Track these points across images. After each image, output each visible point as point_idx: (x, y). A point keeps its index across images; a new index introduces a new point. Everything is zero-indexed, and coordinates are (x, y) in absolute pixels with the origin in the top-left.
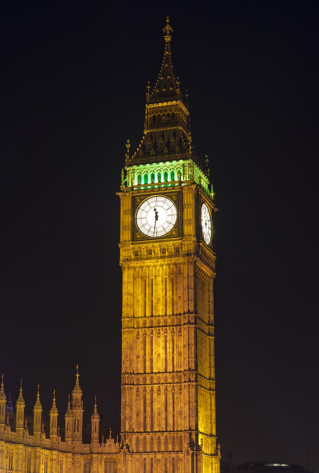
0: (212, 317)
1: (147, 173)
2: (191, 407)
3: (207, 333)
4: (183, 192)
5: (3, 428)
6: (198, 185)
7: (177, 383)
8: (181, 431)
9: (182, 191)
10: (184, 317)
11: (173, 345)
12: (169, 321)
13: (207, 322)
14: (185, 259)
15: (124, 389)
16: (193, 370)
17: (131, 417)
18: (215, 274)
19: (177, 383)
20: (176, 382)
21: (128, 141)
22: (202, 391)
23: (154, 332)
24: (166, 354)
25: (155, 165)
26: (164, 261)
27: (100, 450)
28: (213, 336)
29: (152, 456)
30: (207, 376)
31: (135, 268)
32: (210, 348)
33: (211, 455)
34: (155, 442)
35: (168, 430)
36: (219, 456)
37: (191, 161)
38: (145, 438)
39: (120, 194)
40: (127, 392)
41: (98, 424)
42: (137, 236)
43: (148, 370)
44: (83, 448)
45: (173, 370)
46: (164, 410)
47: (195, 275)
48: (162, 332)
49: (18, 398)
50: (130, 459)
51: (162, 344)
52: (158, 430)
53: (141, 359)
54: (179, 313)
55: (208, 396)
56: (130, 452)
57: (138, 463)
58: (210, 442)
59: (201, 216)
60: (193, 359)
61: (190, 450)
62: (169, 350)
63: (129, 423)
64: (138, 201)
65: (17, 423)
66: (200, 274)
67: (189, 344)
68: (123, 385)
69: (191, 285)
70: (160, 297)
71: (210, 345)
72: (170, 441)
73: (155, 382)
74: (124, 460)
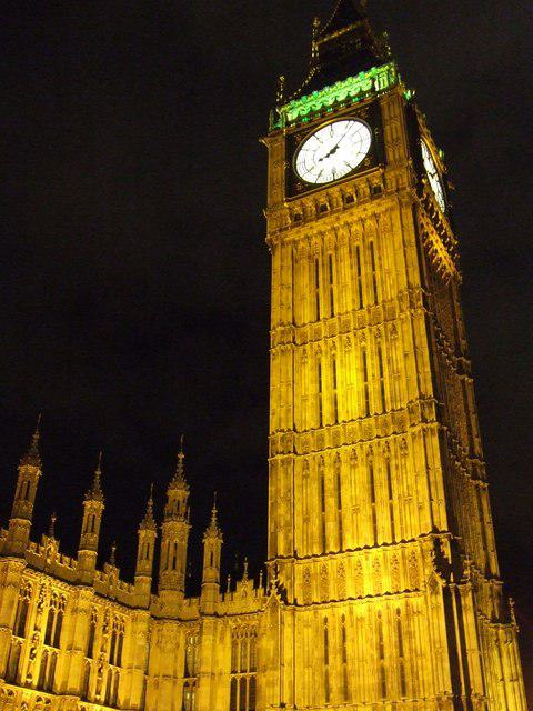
14: (393, 200)
16: (430, 397)
17: (290, 525)
23: (338, 345)
24: (366, 380)
26: (352, 214)
27: (221, 609)
29: (342, 609)
31: (295, 243)
32: (466, 397)
38: (324, 570)
39: (268, 139)
40: (281, 469)
41: (217, 550)
42: (295, 186)
43: (327, 419)
50: (288, 619)
52: (356, 546)
53: (311, 401)
56: (287, 604)
60: (429, 376)
62: (372, 370)
63: (286, 537)
68: (273, 456)
73: (342, 441)
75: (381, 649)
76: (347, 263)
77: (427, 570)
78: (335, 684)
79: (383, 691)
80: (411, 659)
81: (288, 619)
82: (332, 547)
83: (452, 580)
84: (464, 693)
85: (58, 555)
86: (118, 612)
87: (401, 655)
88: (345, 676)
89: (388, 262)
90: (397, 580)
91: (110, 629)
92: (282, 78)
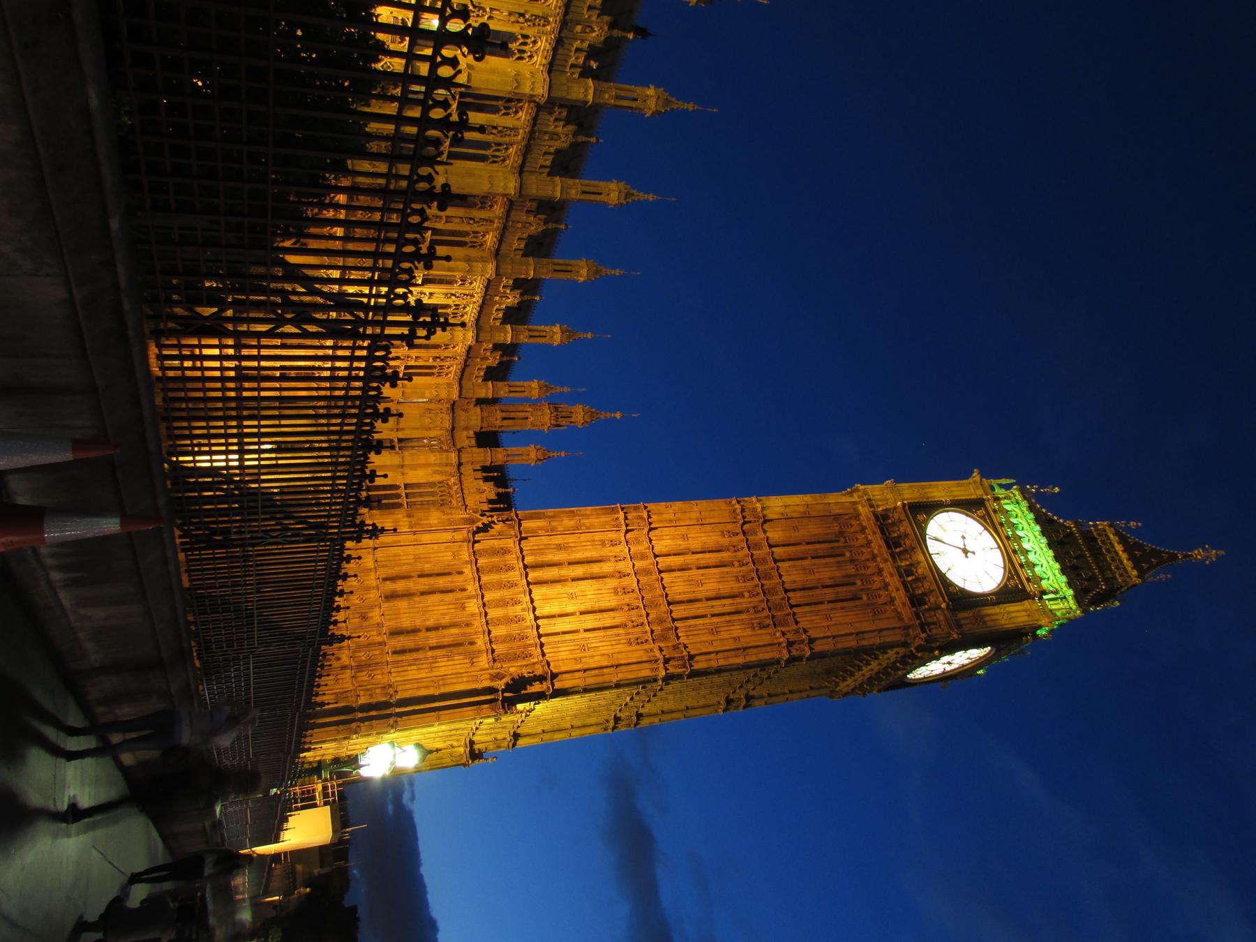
10: (797, 632)
11: (729, 614)
15: (614, 511)
17: (552, 532)
27: (467, 470)
29: (472, 588)
38: (510, 568)
39: (978, 479)
46: (583, 608)
56: (474, 533)
58: (500, 737)
60: (714, 664)
61: (505, 680)
63: (539, 528)
67: (745, 649)
72: (513, 629)
73: (643, 580)
75: (436, 628)
76: (837, 574)
77: (515, 669)
78: (400, 586)
79: (396, 633)
80: (426, 658)
81: (459, 536)
82: (533, 575)
83: (506, 695)
84: (398, 710)
85: (503, 307)
86: (455, 368)
87: (431, 648)
88: (408, 595)
89: (838, 617)
90: (504, 641)
91: (438, 363)
92: (1057, 490)
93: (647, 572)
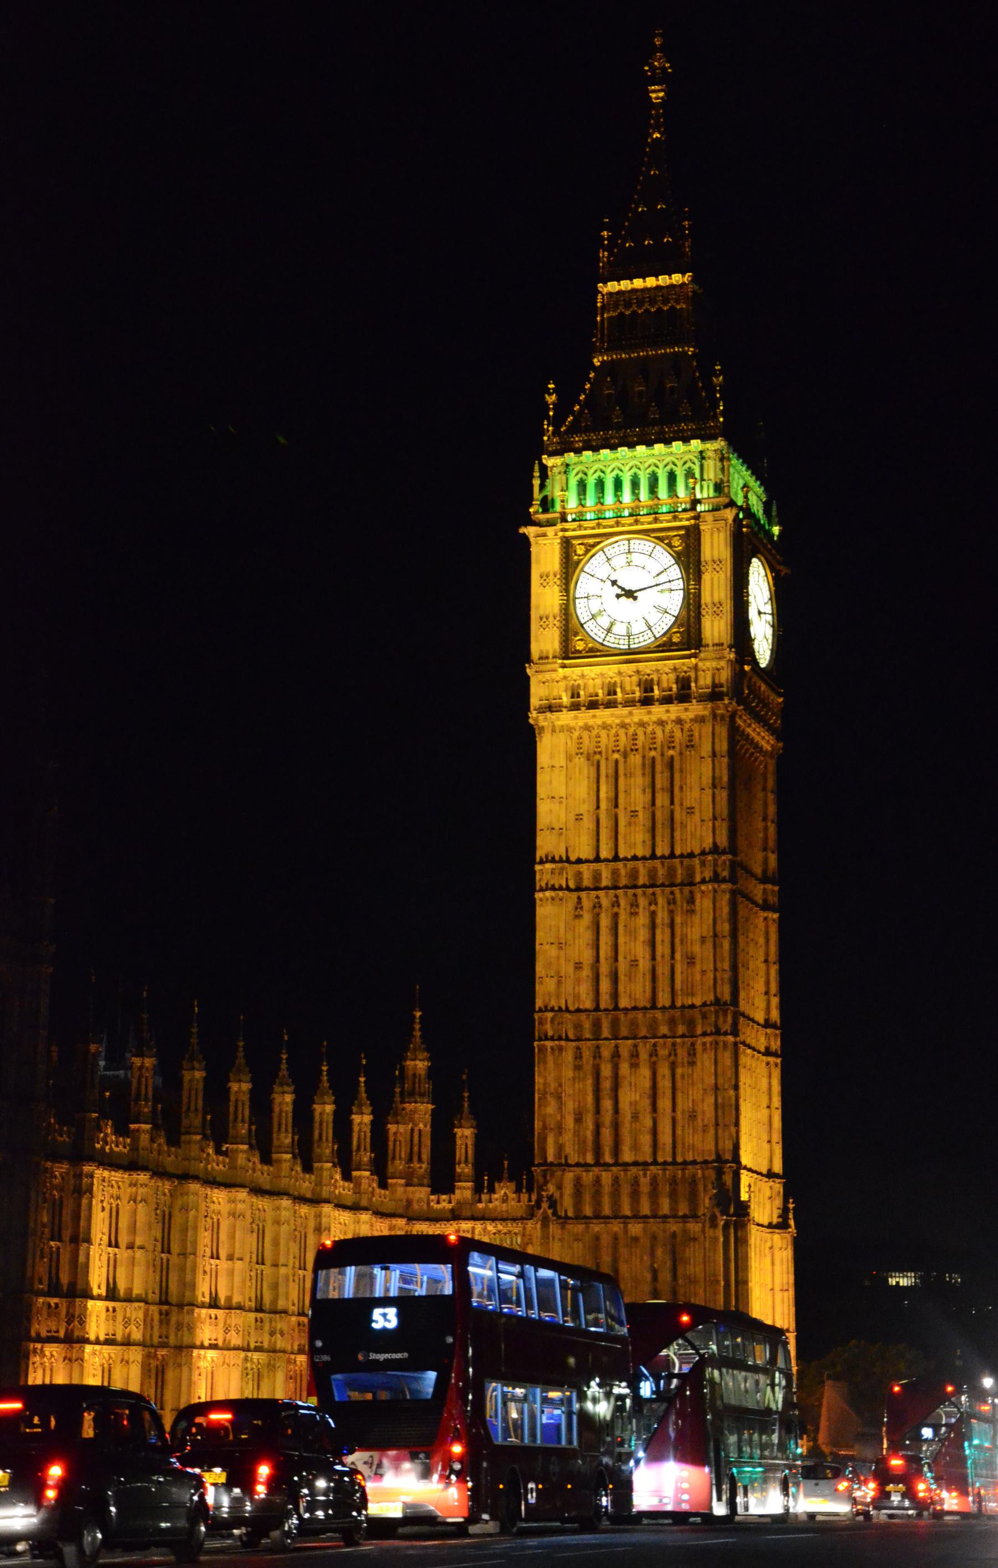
0: (773, 858)
1: (602, 475)
2: (720, 1101)
3: (761, 902)
4: (702, 528)
5: (197, 1146)
6: (740, 508)
7: (683, 1036)
8: (694, 1163)
9: (698, 525)
10: (703, 864)
12: (661, 872)
13: (758, 870)
14: (705, 709)
15: (542, 1049)
16: (725, 1004)
17: (560, 1129)
18: (780, 745)
19: (683, 1036)
20: (680, 1032)
21: (550, 386)
22: (747, 1057)
24: (653, 958)
25: (623, 453)
28: (775, 912)
29: (616, 1227)
30: (760, 1017)
31: (570, 729)
32: (767, 941)
33: (770, 1226)
34: (625, 1190)
35: (660, 1160)
36: (792, 1229)
37: (723, 443)
38: (598, 1181)
39: (530, 531)
40: (550, 1059)
43: (605, 1001)
44: (432, 1204)
45: (673, 1002)
47: (733, 752)
48: (642, 902)
49: (277, 1075)
51: (643, 934)
53: (586, 972)
54: (689, 851)
55: (762, 1070)
56: (559, 1217)
57: (581, 1244)
58: (768, 1193)
59: (747, 592)
60: (727, 976)
61: (718, 1215)
62: (663, 949)
63: (556, 1142)
64: (580, 552)
65: (276, 1143)
66: (743, 746)
67: (715, 935)
68: (540, 1040)
69: (721, 778)
70: (637, 809)
71: (767, 934)
72: (665, 1189)
74: (542, 1238)
75: (655, 1273)
82: (608, 1158)
93: (615, 1024)
